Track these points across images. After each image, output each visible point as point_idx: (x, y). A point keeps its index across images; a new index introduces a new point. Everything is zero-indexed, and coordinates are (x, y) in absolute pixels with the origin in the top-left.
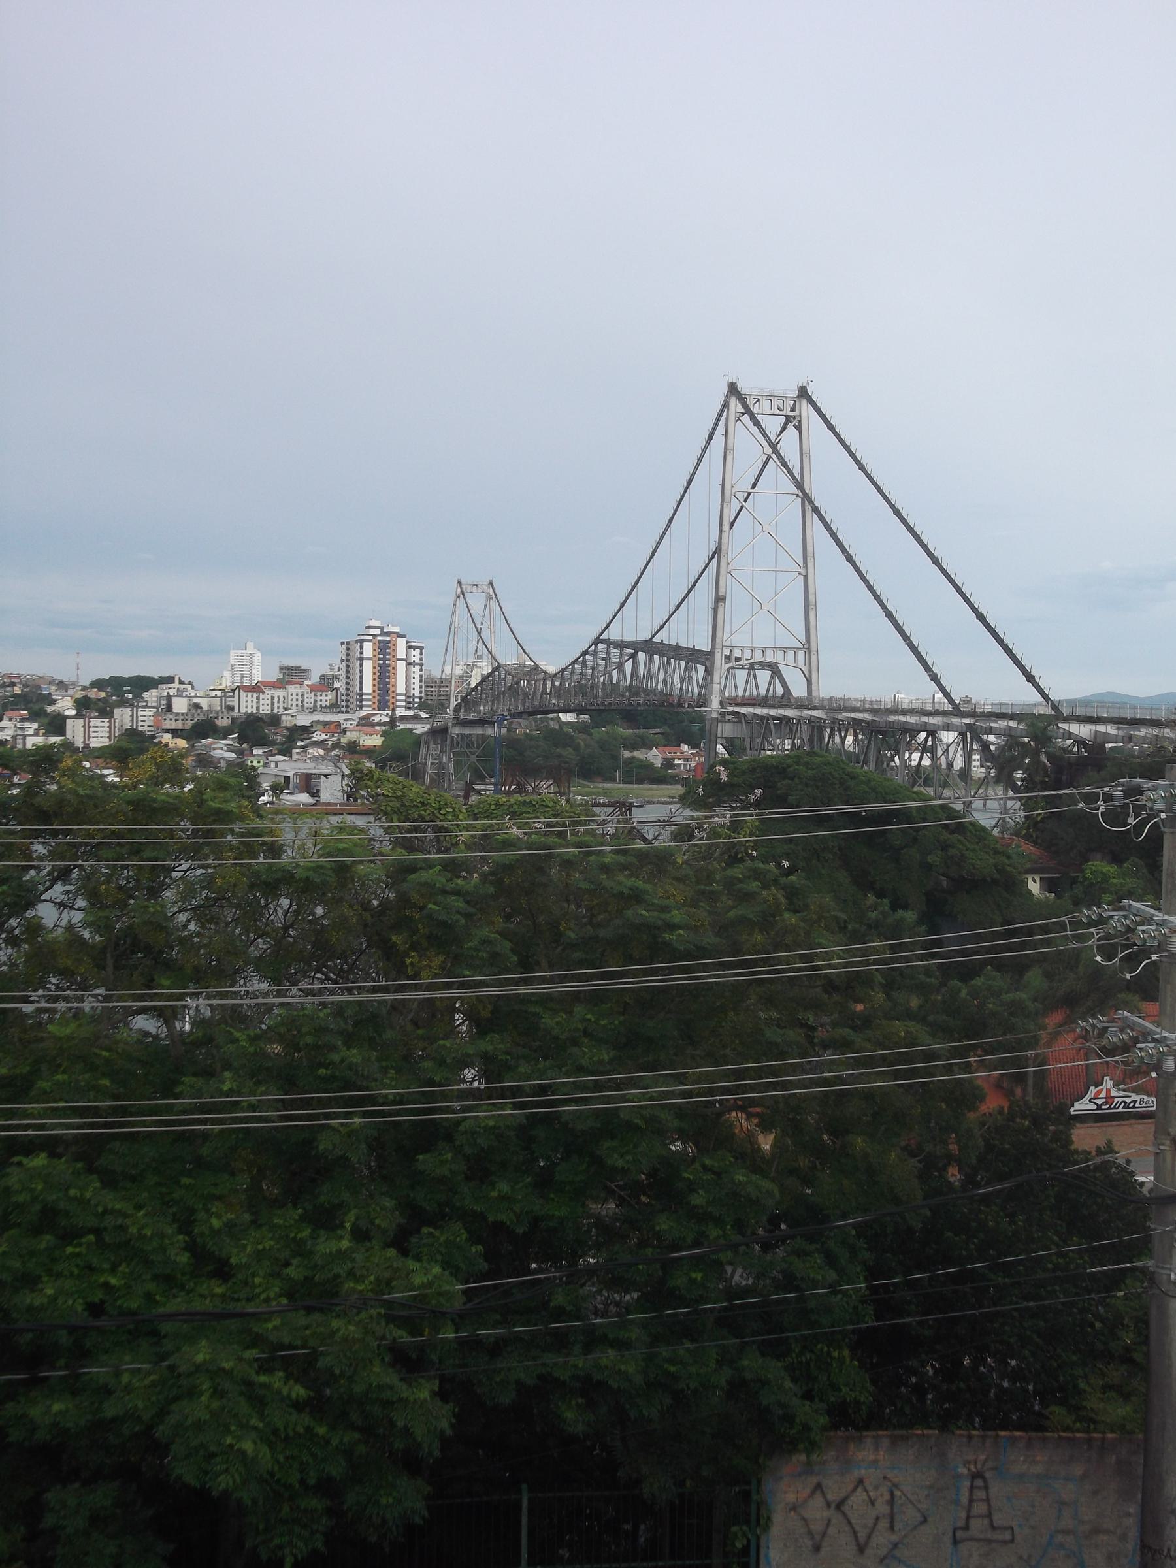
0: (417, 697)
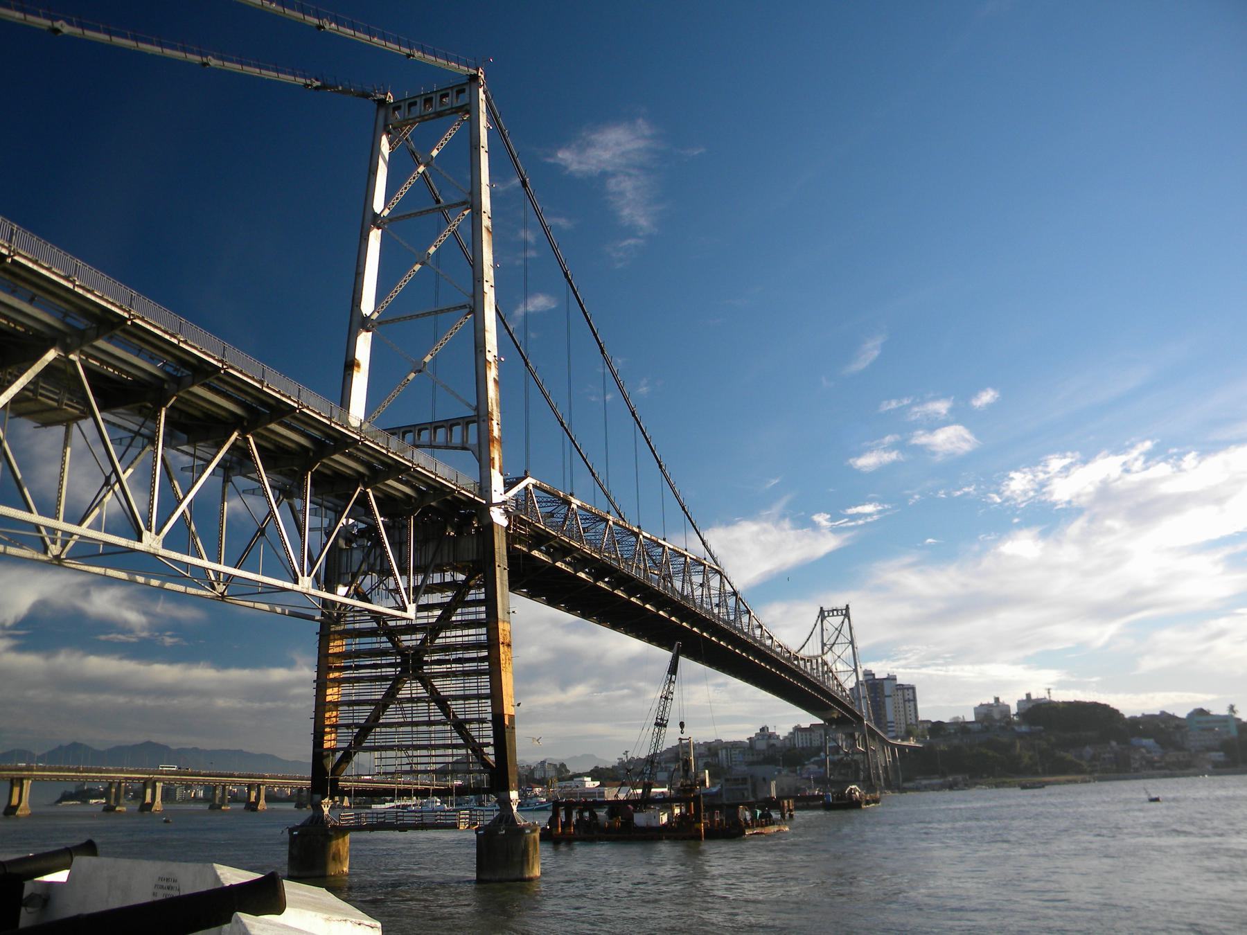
0: (914, 725)
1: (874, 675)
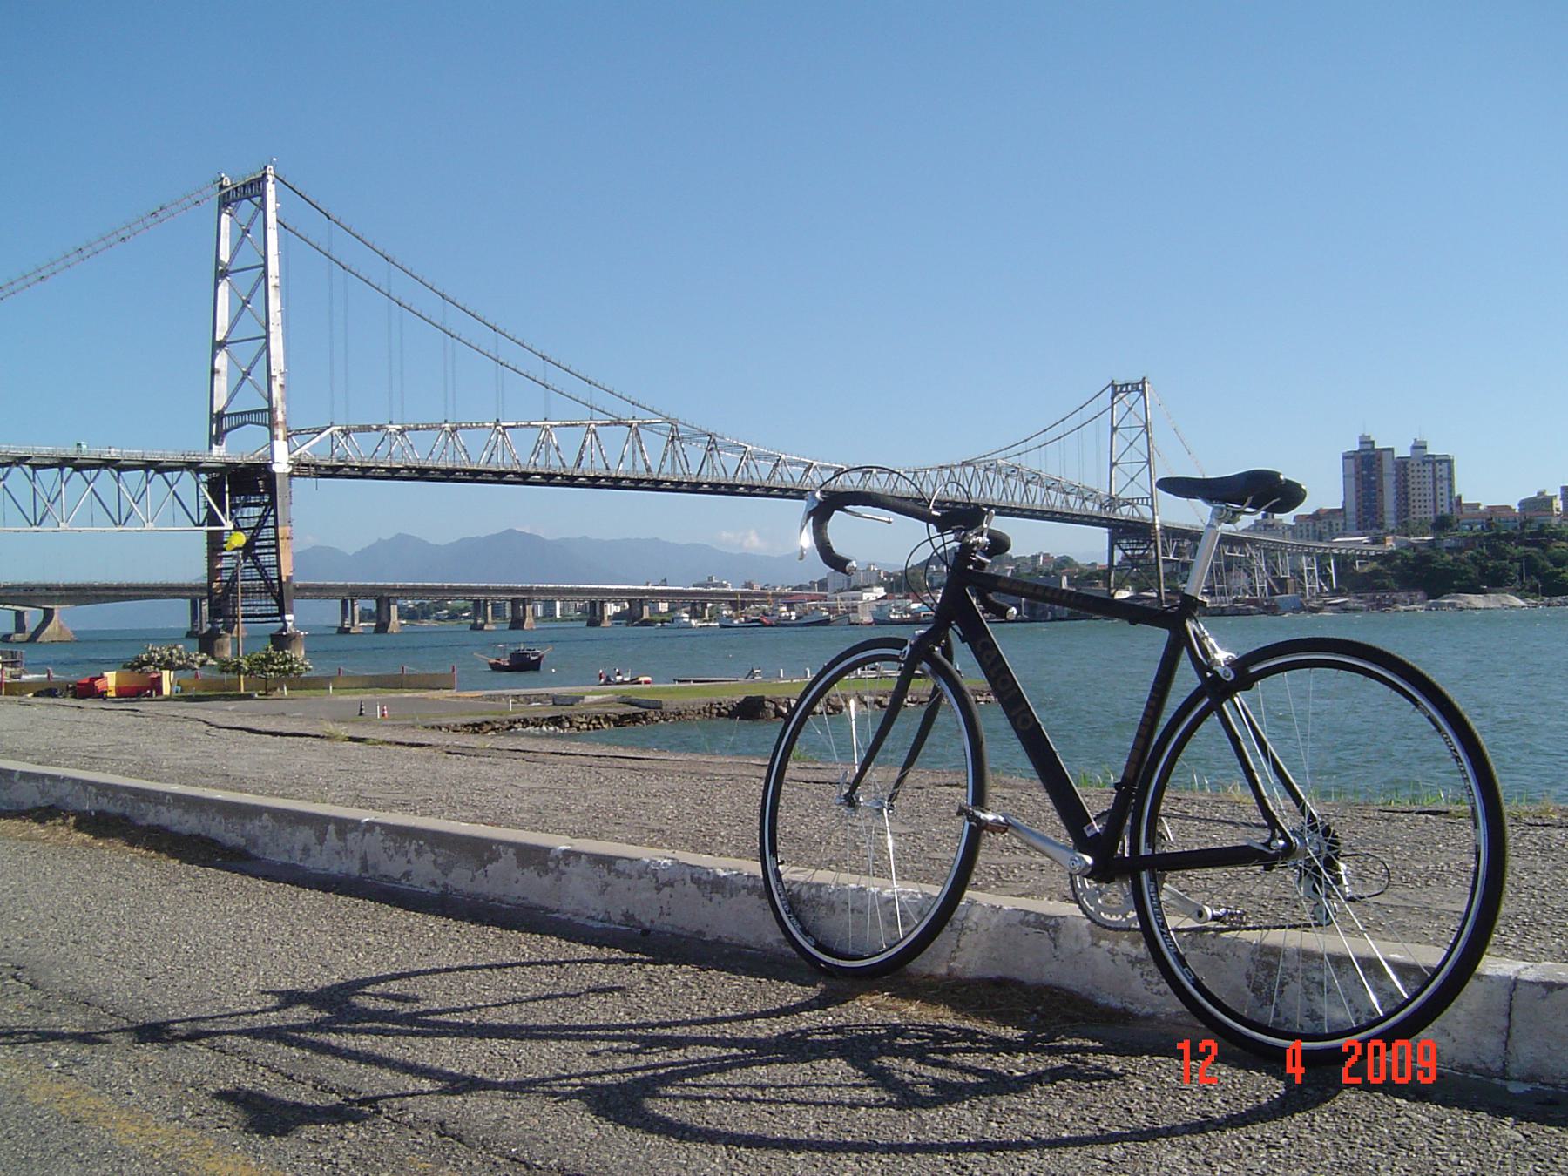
1: (1373, 442)
